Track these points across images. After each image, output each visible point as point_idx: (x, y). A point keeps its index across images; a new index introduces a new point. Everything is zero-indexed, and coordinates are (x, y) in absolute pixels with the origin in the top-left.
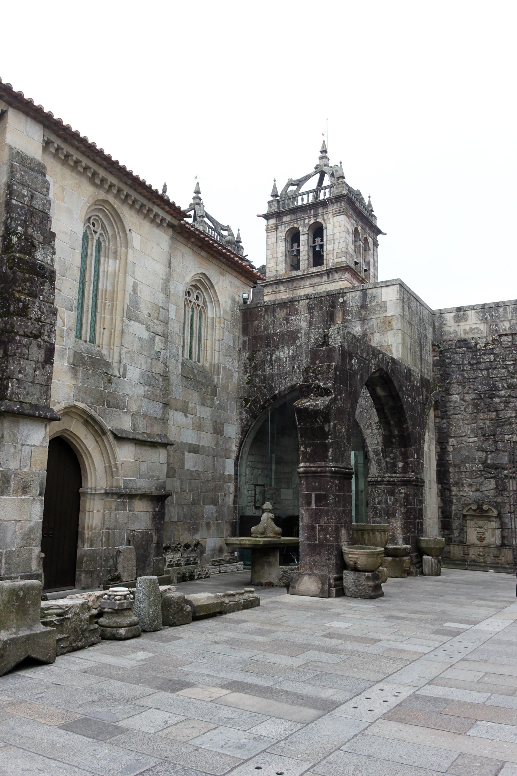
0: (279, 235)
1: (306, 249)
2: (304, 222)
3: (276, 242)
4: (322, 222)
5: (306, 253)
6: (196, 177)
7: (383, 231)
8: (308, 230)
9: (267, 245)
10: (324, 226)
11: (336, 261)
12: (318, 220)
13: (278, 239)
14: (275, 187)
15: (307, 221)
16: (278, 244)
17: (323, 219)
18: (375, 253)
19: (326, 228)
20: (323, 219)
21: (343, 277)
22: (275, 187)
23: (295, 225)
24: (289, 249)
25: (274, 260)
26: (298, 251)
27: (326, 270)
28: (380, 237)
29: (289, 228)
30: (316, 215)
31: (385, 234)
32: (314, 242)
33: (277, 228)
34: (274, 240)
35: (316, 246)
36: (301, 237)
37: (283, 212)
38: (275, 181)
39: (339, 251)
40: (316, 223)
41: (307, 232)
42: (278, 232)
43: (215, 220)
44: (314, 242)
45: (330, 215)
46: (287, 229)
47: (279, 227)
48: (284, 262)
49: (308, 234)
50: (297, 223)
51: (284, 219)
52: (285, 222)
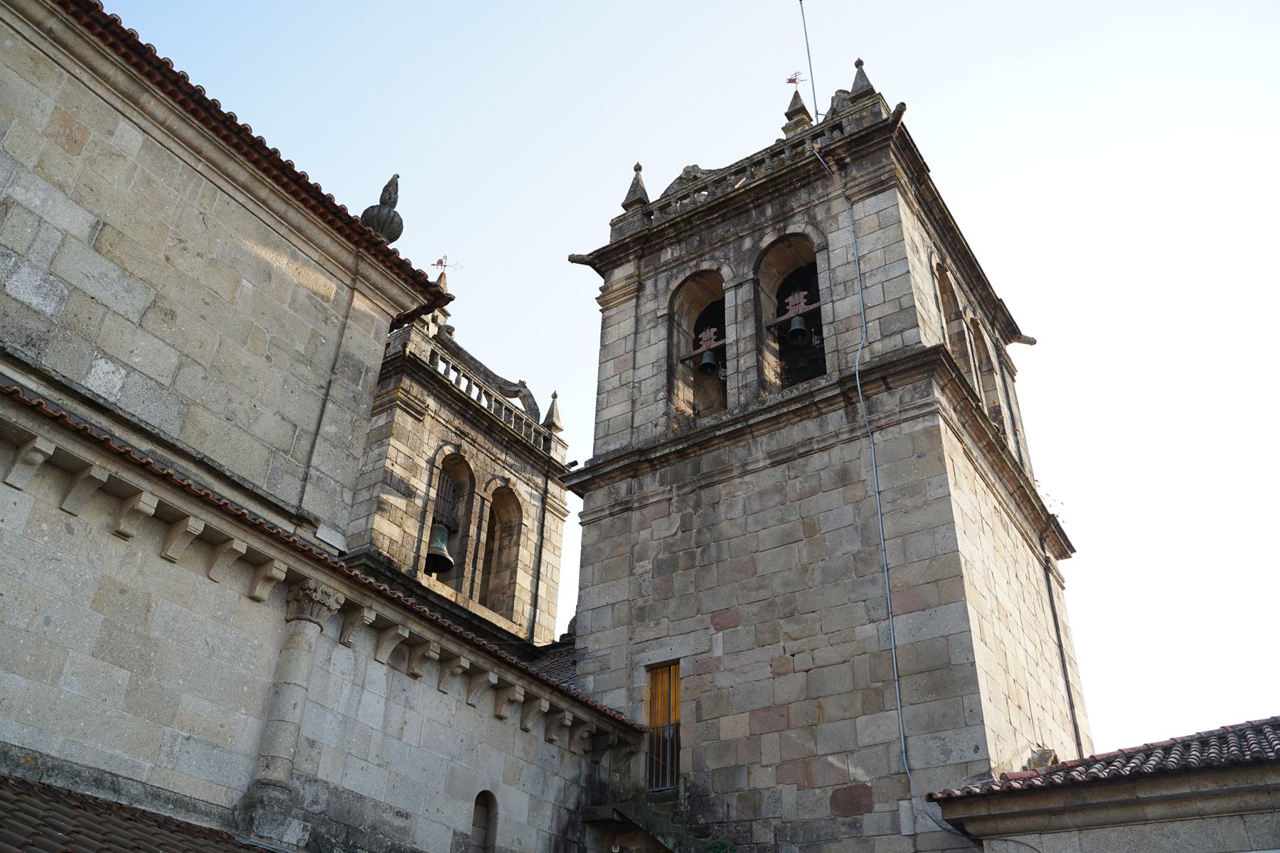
0: (647, 306)
1: (750, 329)
2: (738, 249)
3: (636, 333)
4: (809, 230)
5: (751, 346)
6: (440, 262)
7: (1025, 331)
8: (756, 270)
9: (603, 346)
10: (816, 239)
11: (878, 347)
12: (791, 229)
13: (644, 321)
14: (637, 186)
15: (747, 244)
16: (643, 338)
17: (813, 222)
18: (1011, 394)
19: (825, 247)
20: (813, 222)
21: (920, 402)
22: (637, 186)
23: (705, 266)
24: (684, 349)
25: (624, 394)
26: (720, 353)
27: (841, 382)
28: (1014, 350)
29: (681, 278)
30: (784, 217)
31: (1032, 342)
32: (782, 310)
33: (640, 288)
34: (627, 326)
35: (789, 321)
36: (729, 297)
37: (661, 233)
38: (638, 168)
39: (887, 309)
40: (783, 239)
41: (751, 276)
42: (643, 300)
43: (481, 365)
44: (782, 310)
45: (839, 206)
46: (674, 285)
47: (649, 285)
48: (662, 395)
49: (756, 282)
50: (712, 258)
51: (667, 255)
52: (666, 264)
